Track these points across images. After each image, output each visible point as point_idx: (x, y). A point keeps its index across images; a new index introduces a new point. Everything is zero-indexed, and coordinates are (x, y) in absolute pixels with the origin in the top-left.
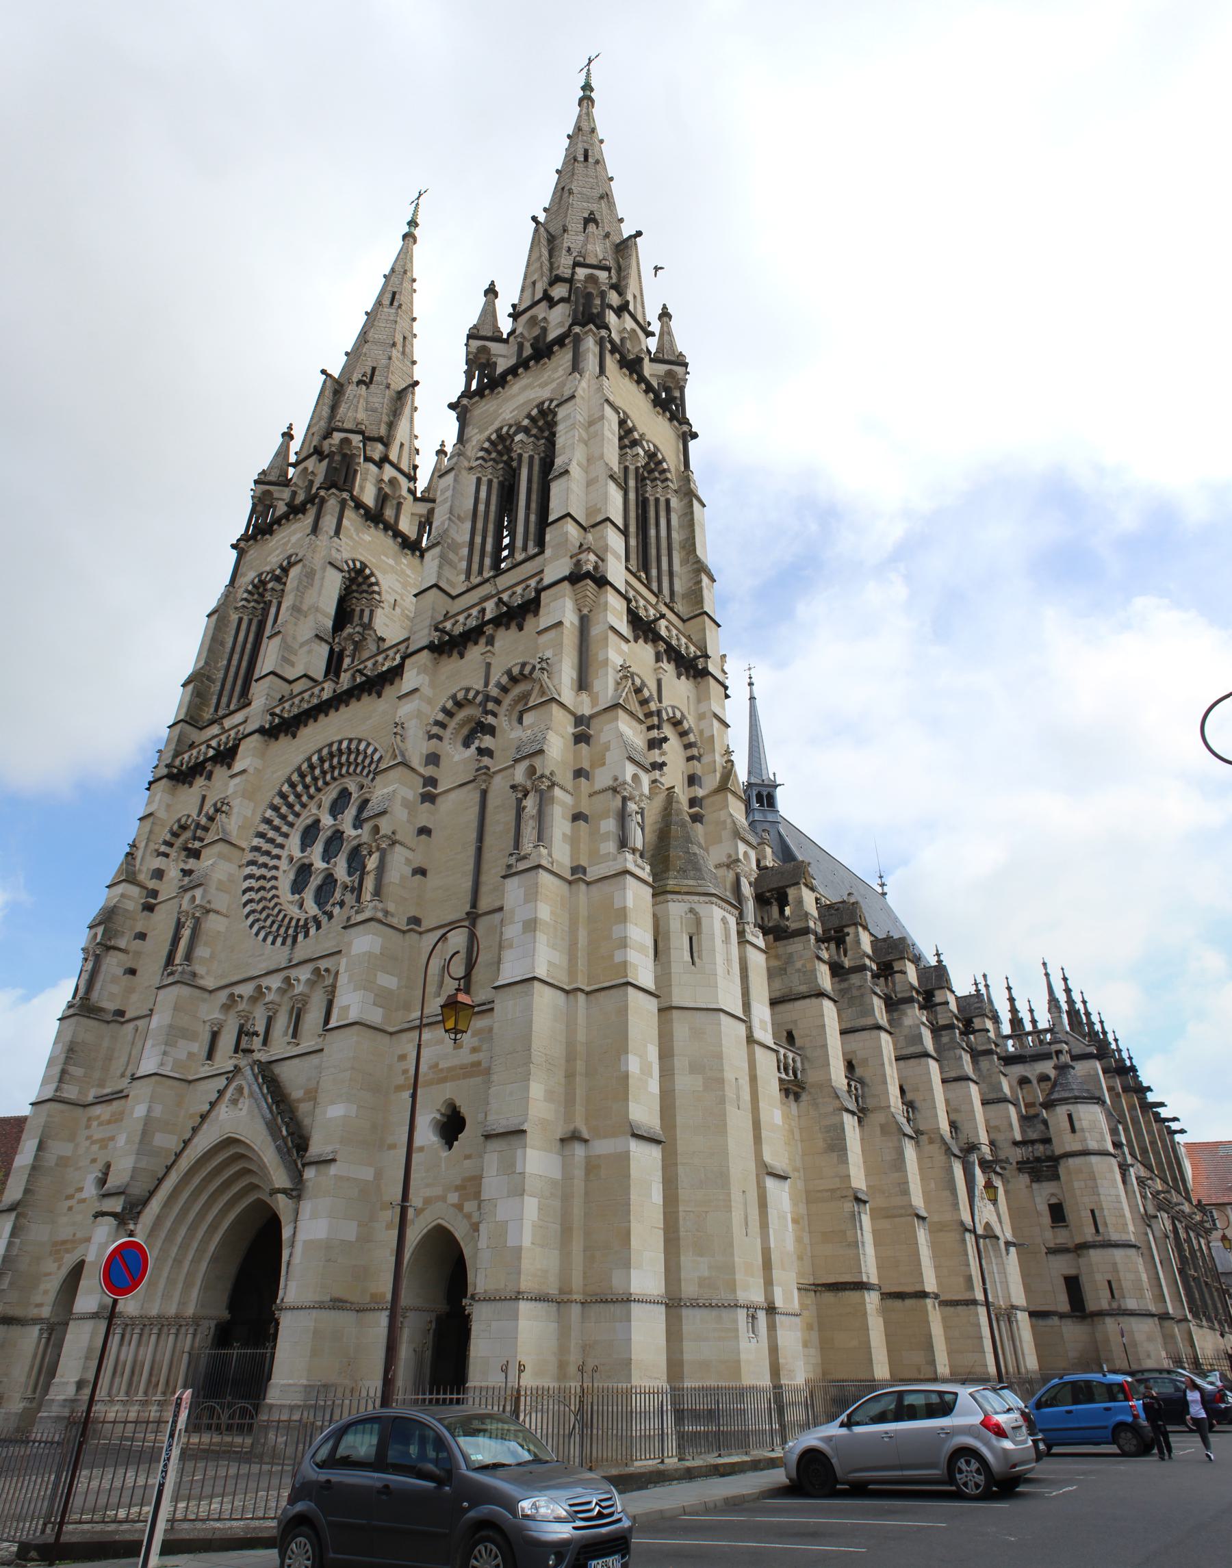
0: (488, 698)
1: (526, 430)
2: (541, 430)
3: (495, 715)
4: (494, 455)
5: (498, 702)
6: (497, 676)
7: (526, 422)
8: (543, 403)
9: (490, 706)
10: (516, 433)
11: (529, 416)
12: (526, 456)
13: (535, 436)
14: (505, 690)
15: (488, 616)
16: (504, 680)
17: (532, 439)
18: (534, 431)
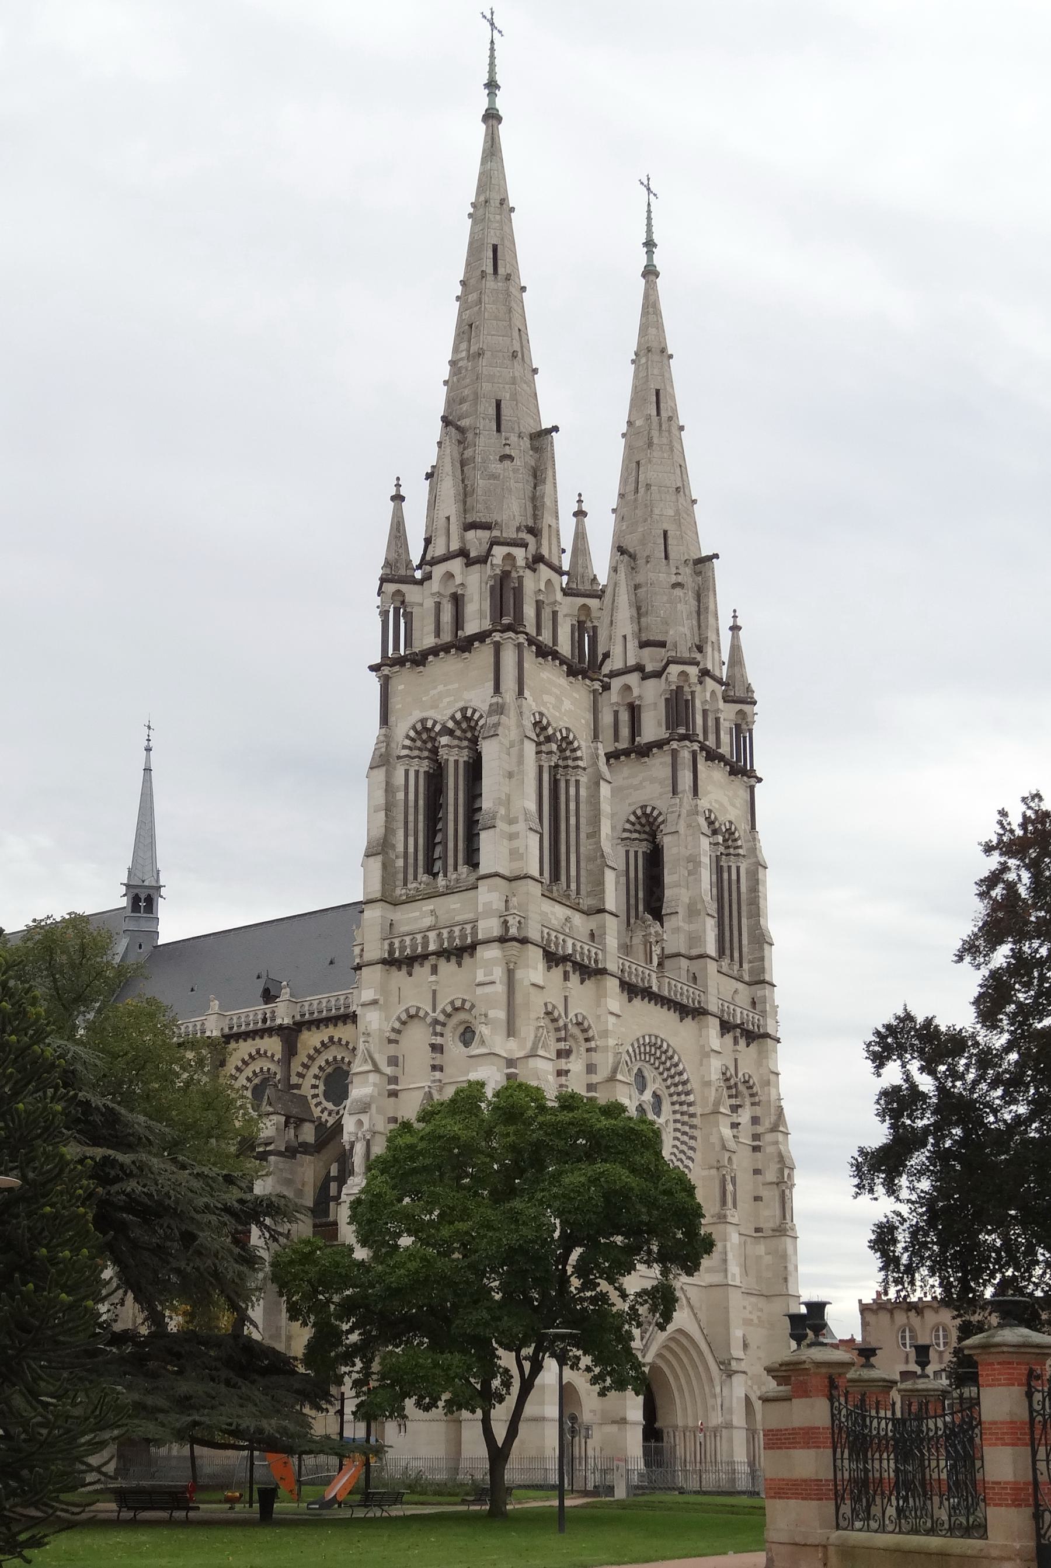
0: (436, 1022)
1: (451, 733)
2: (464, 731)
3: (442, 1035)
4: (419, 743)
5: (444, 1025)
6: (443, 1003)
7: (451, 724)
8: (466, 708)
9: (438, 1028)
10: (441, 733)
11: (453, 718)
12: (452, 759)
13: (460, 739)
14: (449, 1016)
15: (432, 947)
16: (449, 1009)
17: (456, 742)
18: (458, 733)
